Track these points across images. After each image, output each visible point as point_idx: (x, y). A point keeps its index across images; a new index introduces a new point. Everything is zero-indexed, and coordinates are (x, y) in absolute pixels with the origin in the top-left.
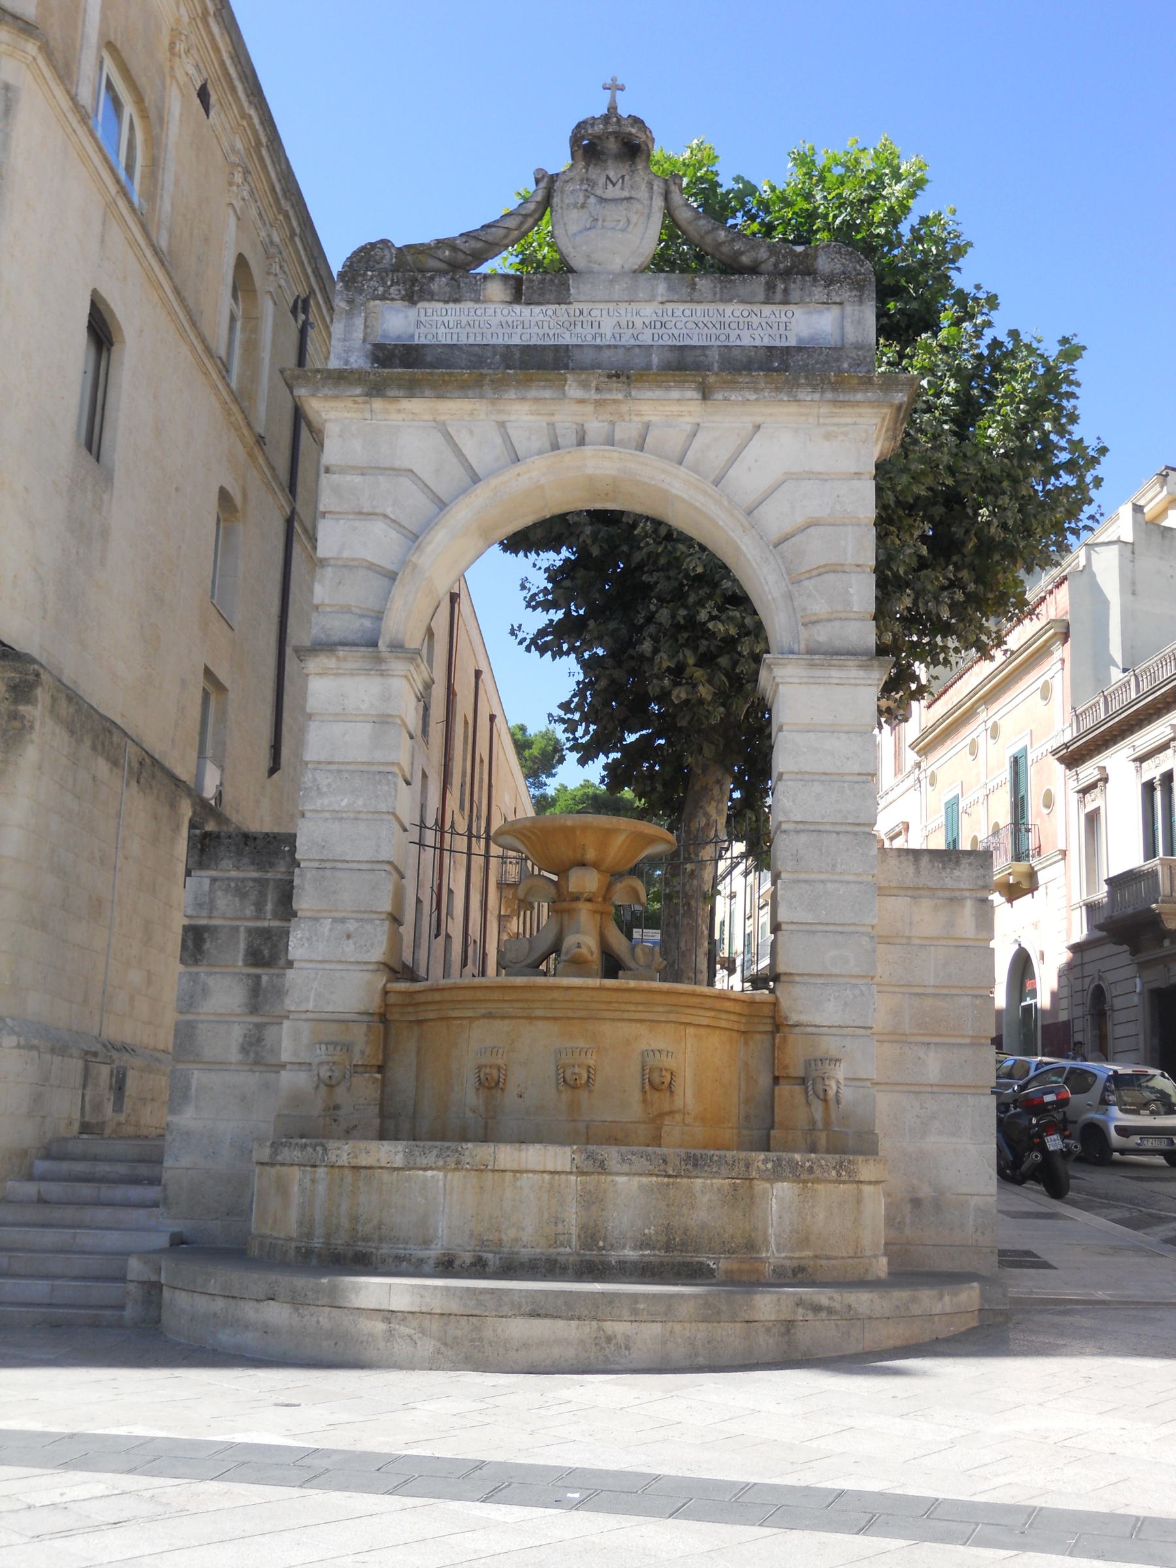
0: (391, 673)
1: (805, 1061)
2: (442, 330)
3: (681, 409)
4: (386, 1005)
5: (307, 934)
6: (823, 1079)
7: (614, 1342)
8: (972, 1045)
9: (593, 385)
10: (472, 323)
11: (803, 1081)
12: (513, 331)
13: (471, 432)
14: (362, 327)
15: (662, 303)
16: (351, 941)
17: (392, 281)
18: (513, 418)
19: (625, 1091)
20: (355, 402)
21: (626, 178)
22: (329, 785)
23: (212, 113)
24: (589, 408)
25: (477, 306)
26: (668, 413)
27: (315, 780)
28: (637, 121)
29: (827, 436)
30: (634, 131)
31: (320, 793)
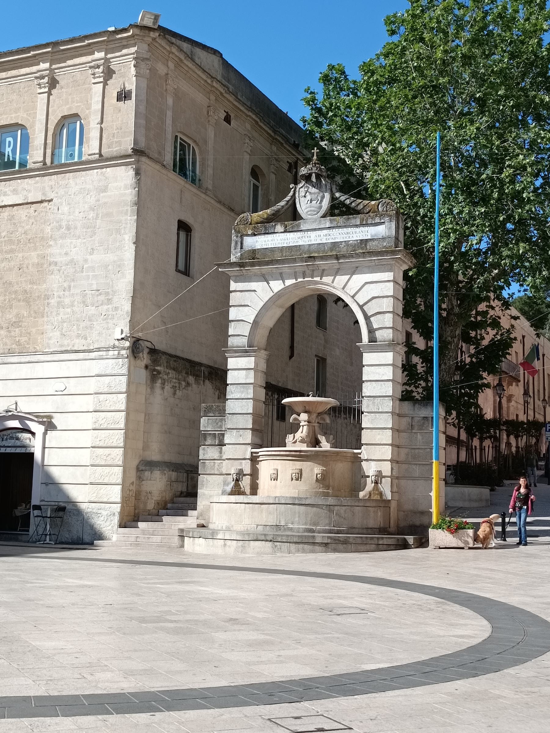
23: (232, 122)
31: (232, 393)
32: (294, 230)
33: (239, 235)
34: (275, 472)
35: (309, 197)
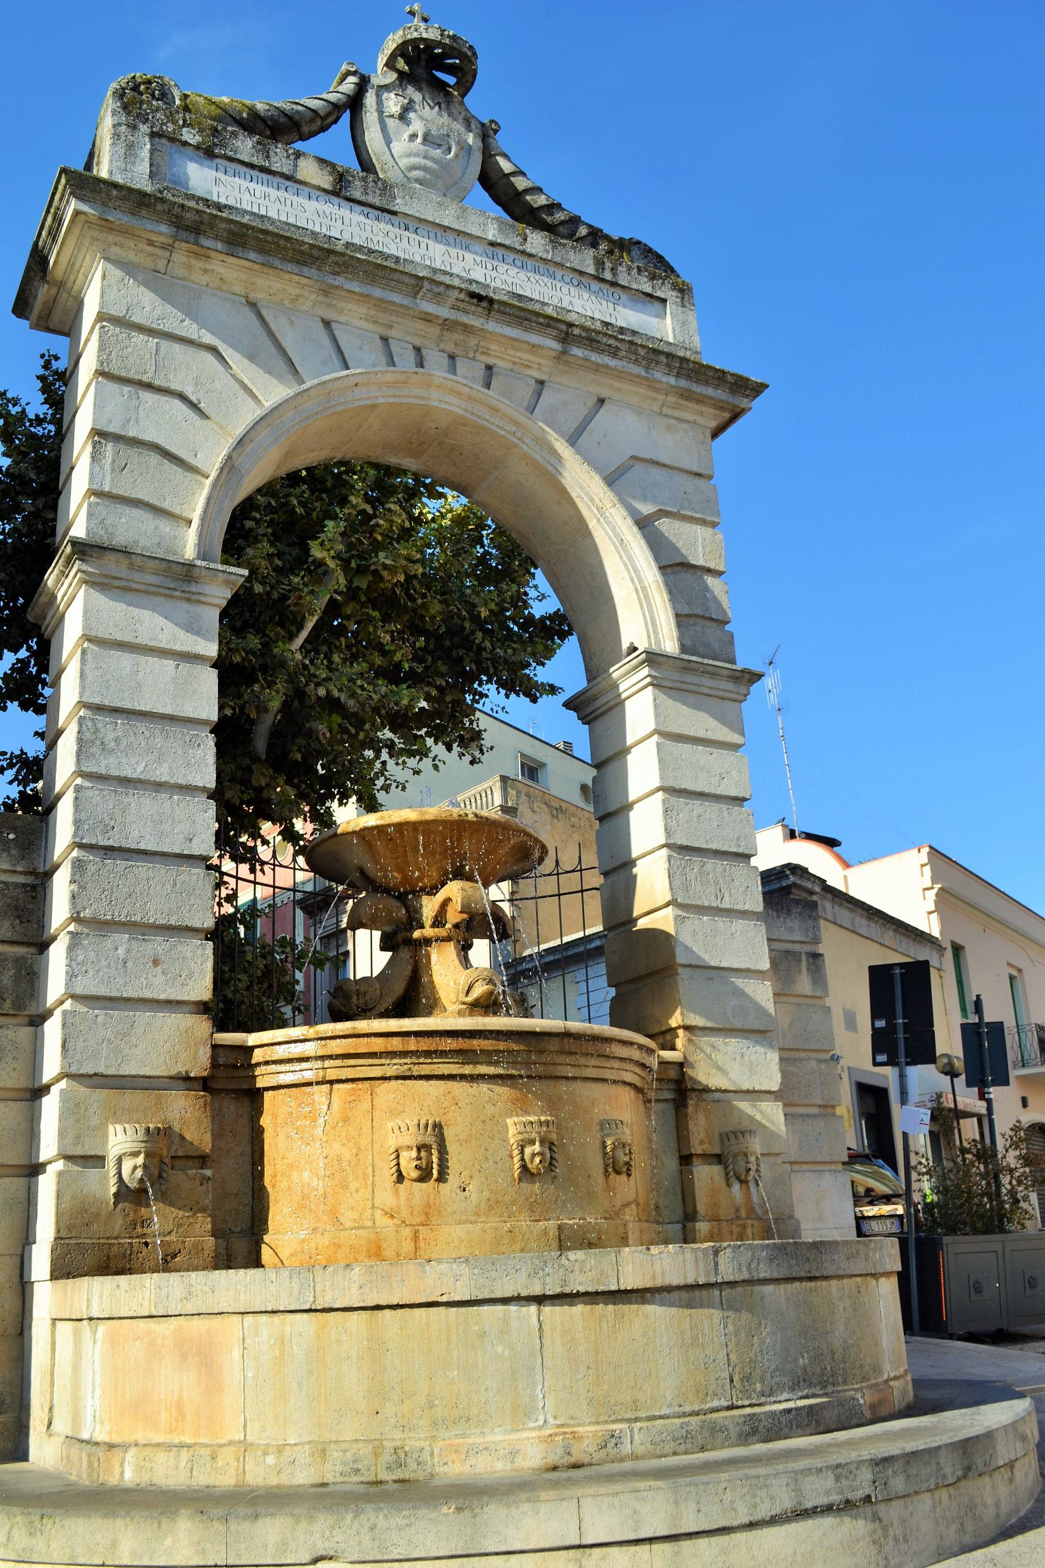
0: (202, 598)
1: (721, 1135)
2: (246, 197)
3: (532, 358)
4: (215, 1064)
5: (92, 955)
6: (746, 1155)
7: (891, 1533)
8: (821, 1115)
9: (451, 301)
10: (283, 200)
11: (718, 1159)
12: (330, 223)
13: (292, 322)
14: (147, 160)
15: (492, 244)
16: (159, 968)
17: (184, 121)
18: (343, 319)
19: (589, 1176)
20: (151, 243)
21: (443, 106)
22: (117, 740)
24: (434, 331)
25: (288, 183)
26: (517, 360)
27: (97, 731)
28: (471, 47)
29: (669, 428)
30: (469, 54)
32: (370, 199)
33: (144, 128)
34: (430, 1140)
35: (417, 126)
